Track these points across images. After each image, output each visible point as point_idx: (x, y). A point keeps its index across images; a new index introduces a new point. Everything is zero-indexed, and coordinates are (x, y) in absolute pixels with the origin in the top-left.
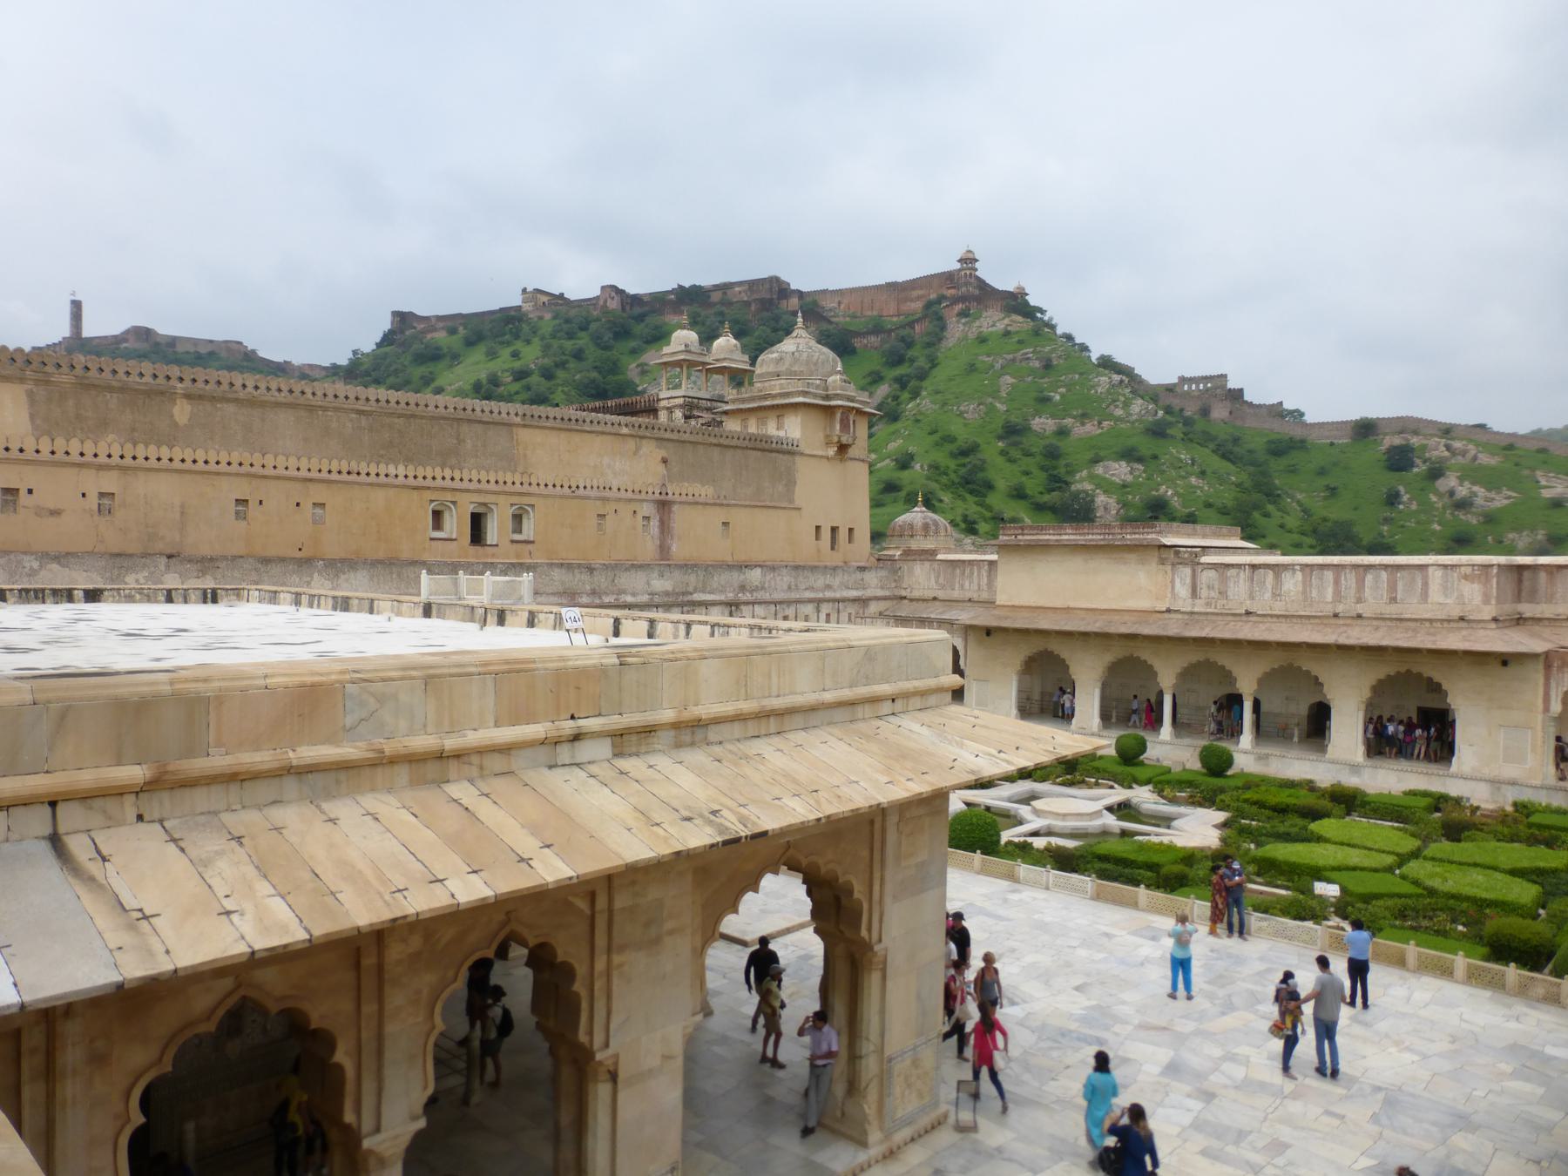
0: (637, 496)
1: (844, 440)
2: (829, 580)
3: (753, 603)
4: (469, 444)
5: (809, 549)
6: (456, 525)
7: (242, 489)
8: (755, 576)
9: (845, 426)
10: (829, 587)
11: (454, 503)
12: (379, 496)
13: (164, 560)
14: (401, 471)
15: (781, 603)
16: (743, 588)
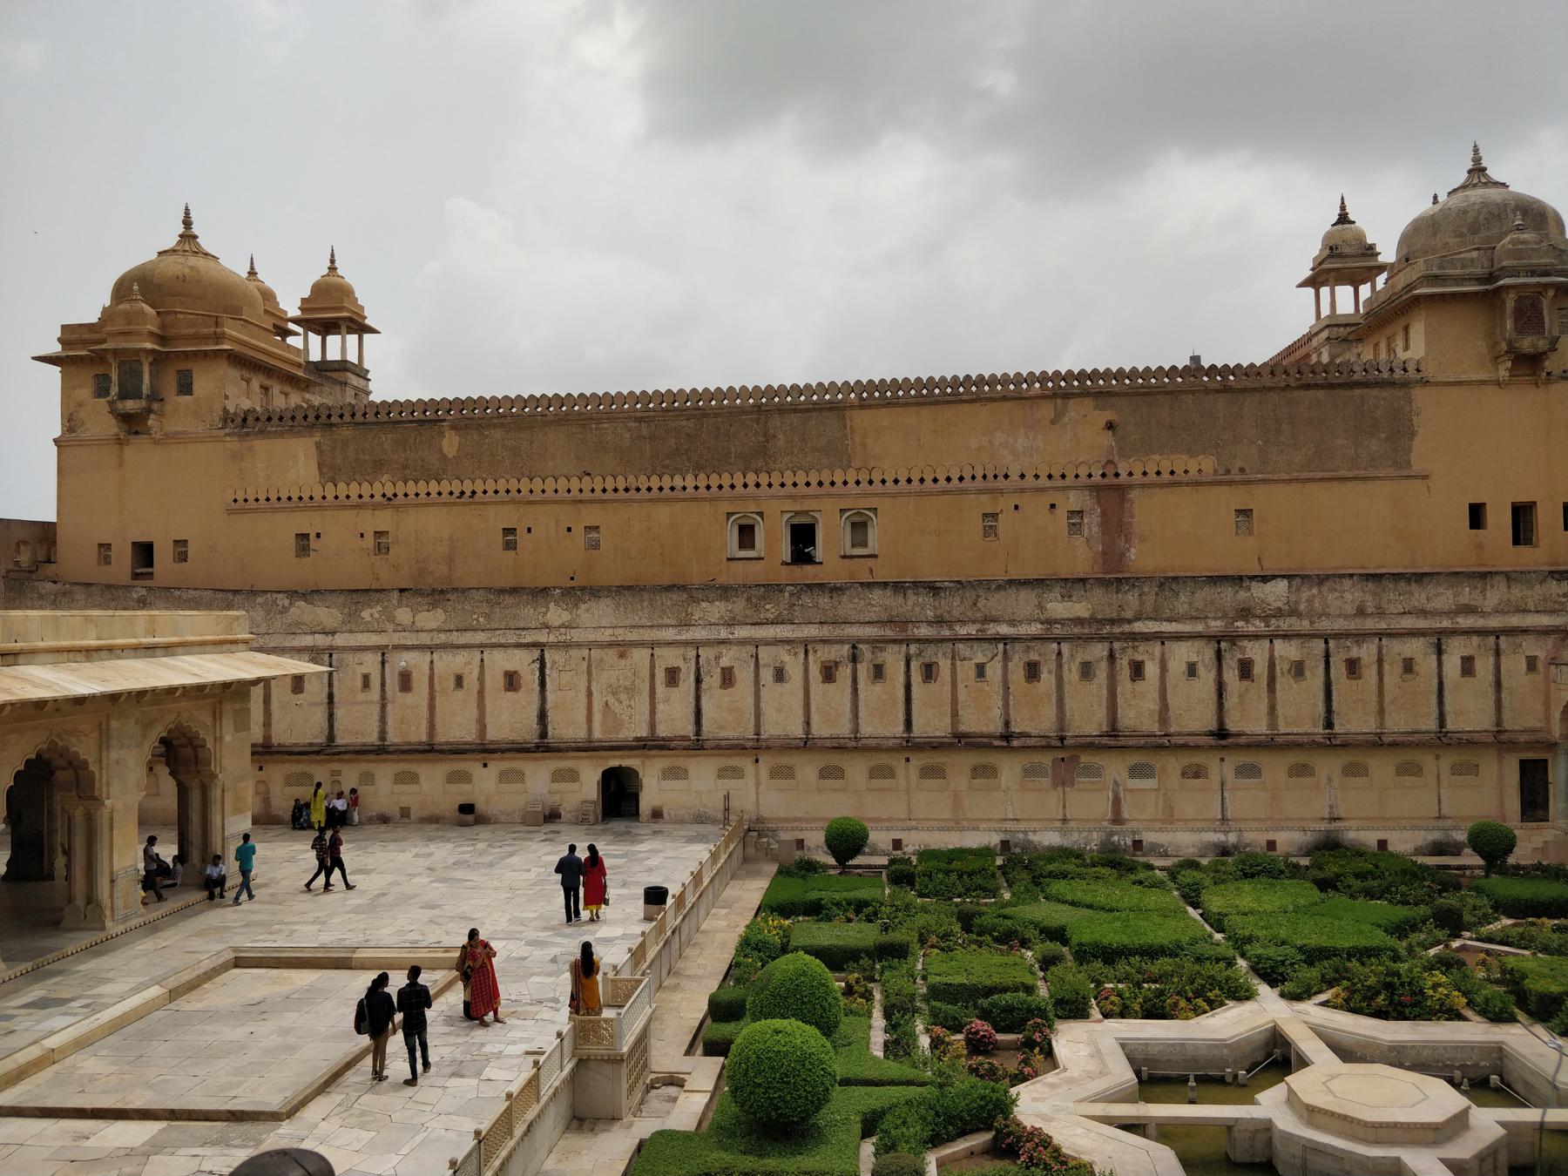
0: (1060, 483)
1: (1527, 344)
2: (1466, 595)
3: (1271, 638)
4: (781, 441)
5: (1451, 541)
6: (774, 541)
7: (508, 516)
8: (1276, 593)
9: (1528, 315)
10: (1469, 610)
11: (761, 514)
12: (662, 514)
13: (396, 594)
14: (690, 481)
15: (1338, 636)
16: (1245, 613)
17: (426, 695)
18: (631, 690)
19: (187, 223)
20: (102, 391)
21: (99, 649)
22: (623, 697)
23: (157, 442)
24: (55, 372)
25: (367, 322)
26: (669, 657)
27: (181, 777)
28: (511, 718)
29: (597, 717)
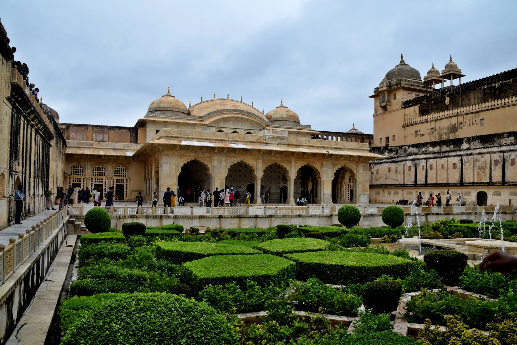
18: (484, 168)
19: (402, 58)
21: (320, 147)
22: (482, 170)
23: (390, 112)
24: (373, 99)
25: (462, 74)
26: (496, 156)
28: (455, 178)
29: (476, 176)
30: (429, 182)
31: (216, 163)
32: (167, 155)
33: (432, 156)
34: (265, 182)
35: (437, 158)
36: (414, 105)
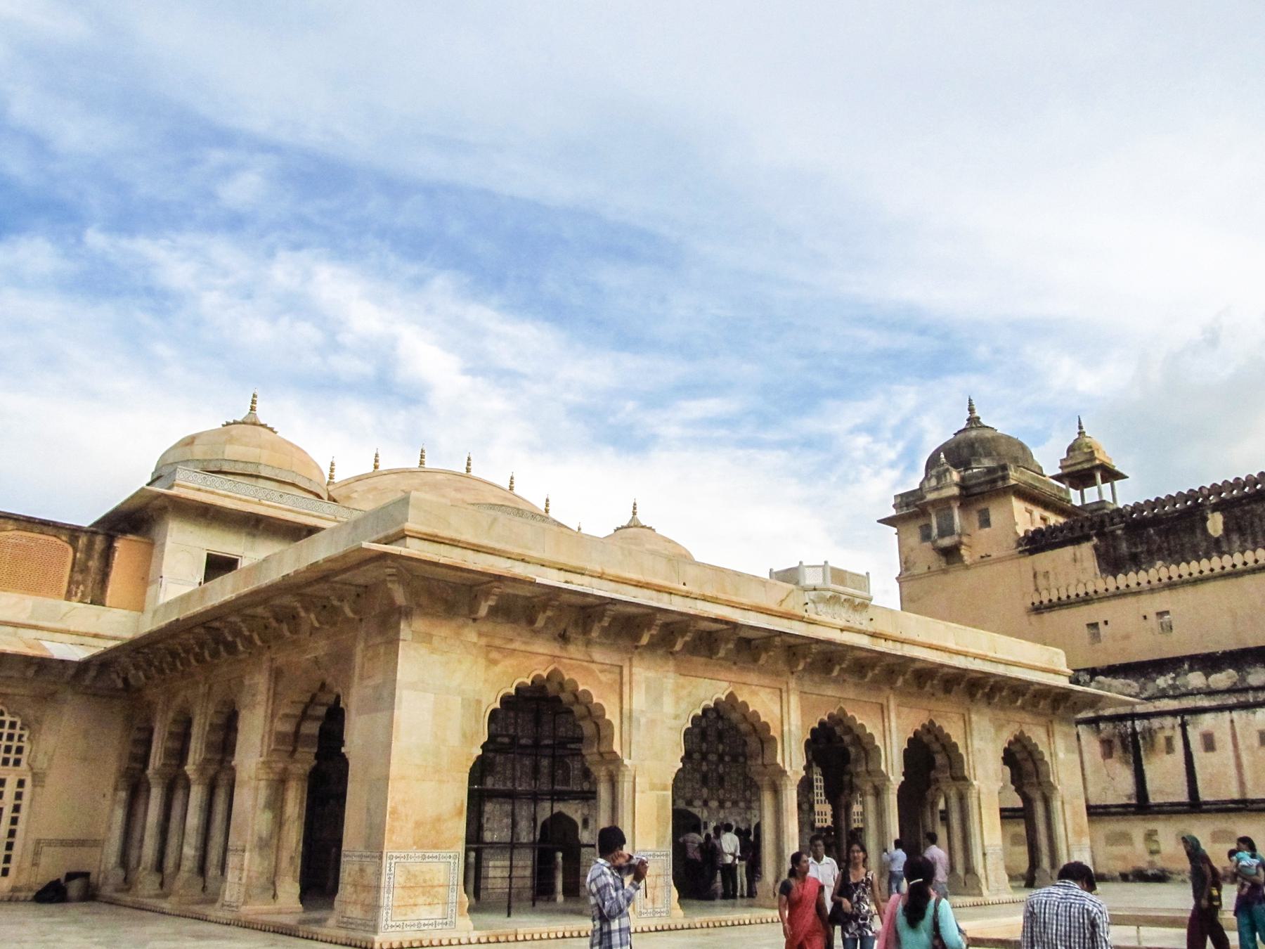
17: (1231, 754)
19: (971, 410)
20: (926, 536)
27: (1026, 789)
30: (1205, 795)
31: (638, 700)
32: (427, 638)
33: (1205, 702)
34: (705, 803)
35: (1231, 708)
36: (1076, 541)
